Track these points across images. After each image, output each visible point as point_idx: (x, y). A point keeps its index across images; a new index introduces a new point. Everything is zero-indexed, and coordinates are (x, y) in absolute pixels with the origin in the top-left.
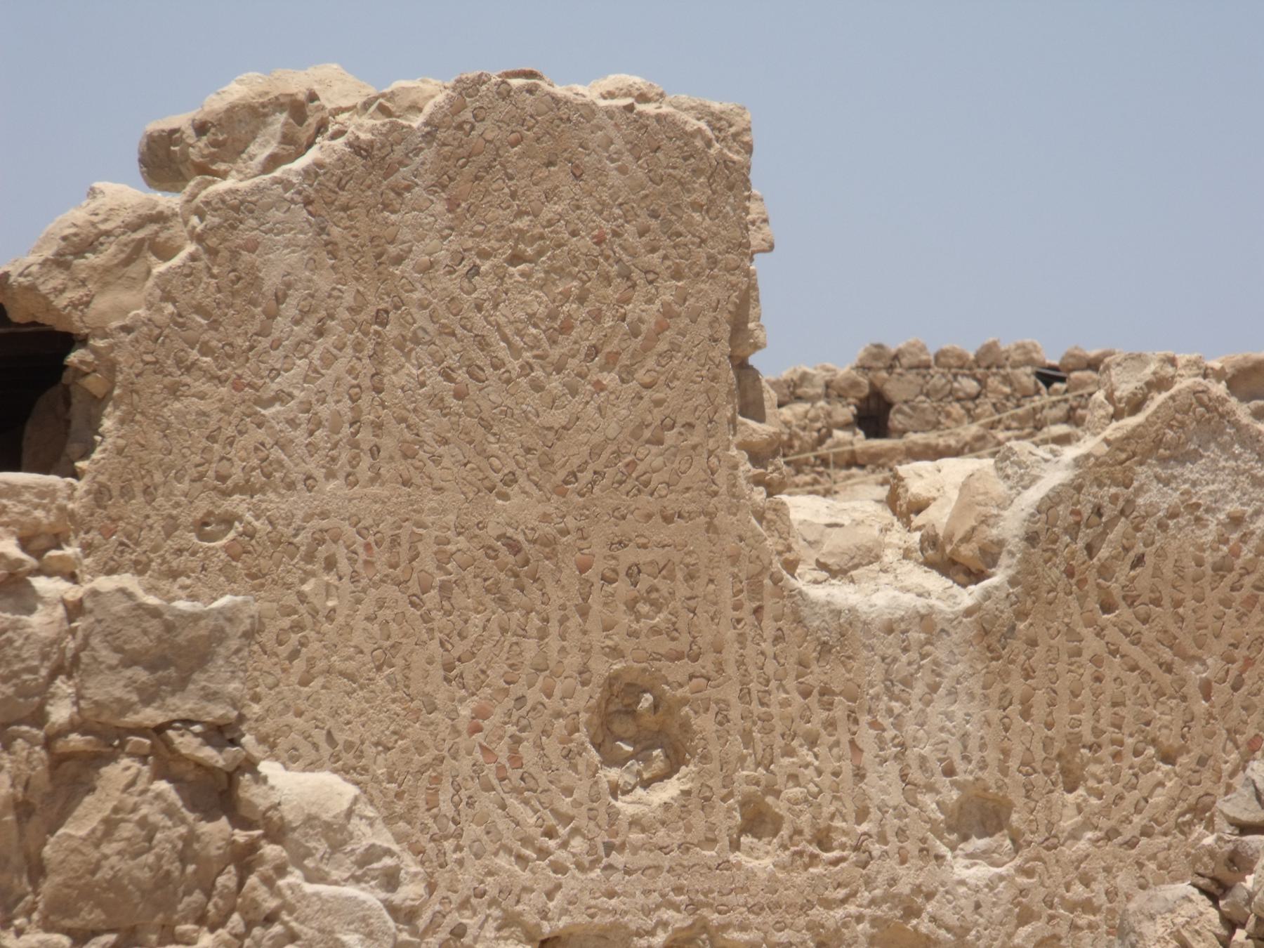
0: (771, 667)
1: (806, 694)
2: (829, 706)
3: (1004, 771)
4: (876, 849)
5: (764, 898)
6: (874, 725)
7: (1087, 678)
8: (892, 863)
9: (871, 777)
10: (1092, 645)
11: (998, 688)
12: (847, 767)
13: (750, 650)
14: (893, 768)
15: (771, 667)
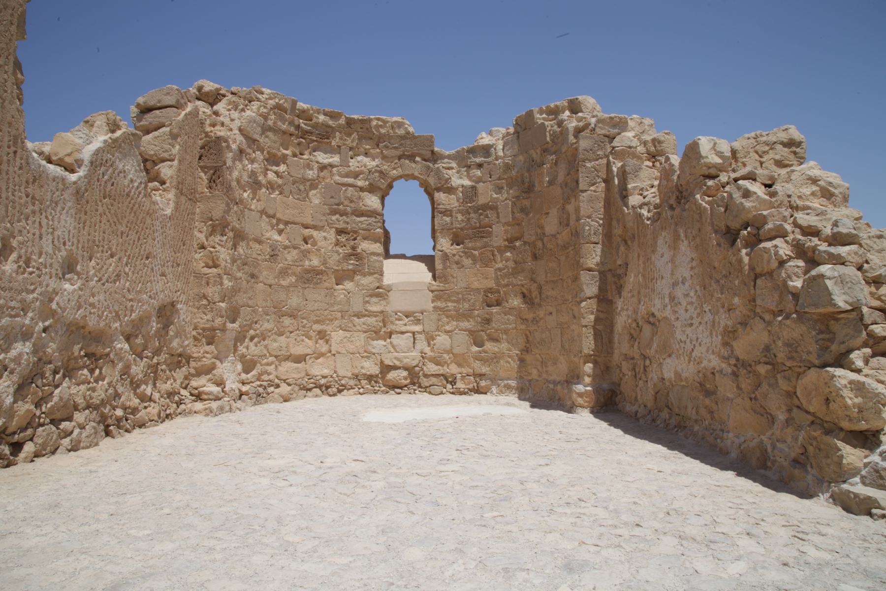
0: (17, 179)
1: (27, 196)
2: (34, 204)
3: (78, 248)
4: (44, 271)
5: (7, 285)
6: (47, 217)
7: (98, 220)
8: (47, 277)
9: (44, 239)
10: (100, 209)
11: (78, 216)
12: (38, 233)
13: (11, 168)
14: (50, 237)
15: (17, 179)
